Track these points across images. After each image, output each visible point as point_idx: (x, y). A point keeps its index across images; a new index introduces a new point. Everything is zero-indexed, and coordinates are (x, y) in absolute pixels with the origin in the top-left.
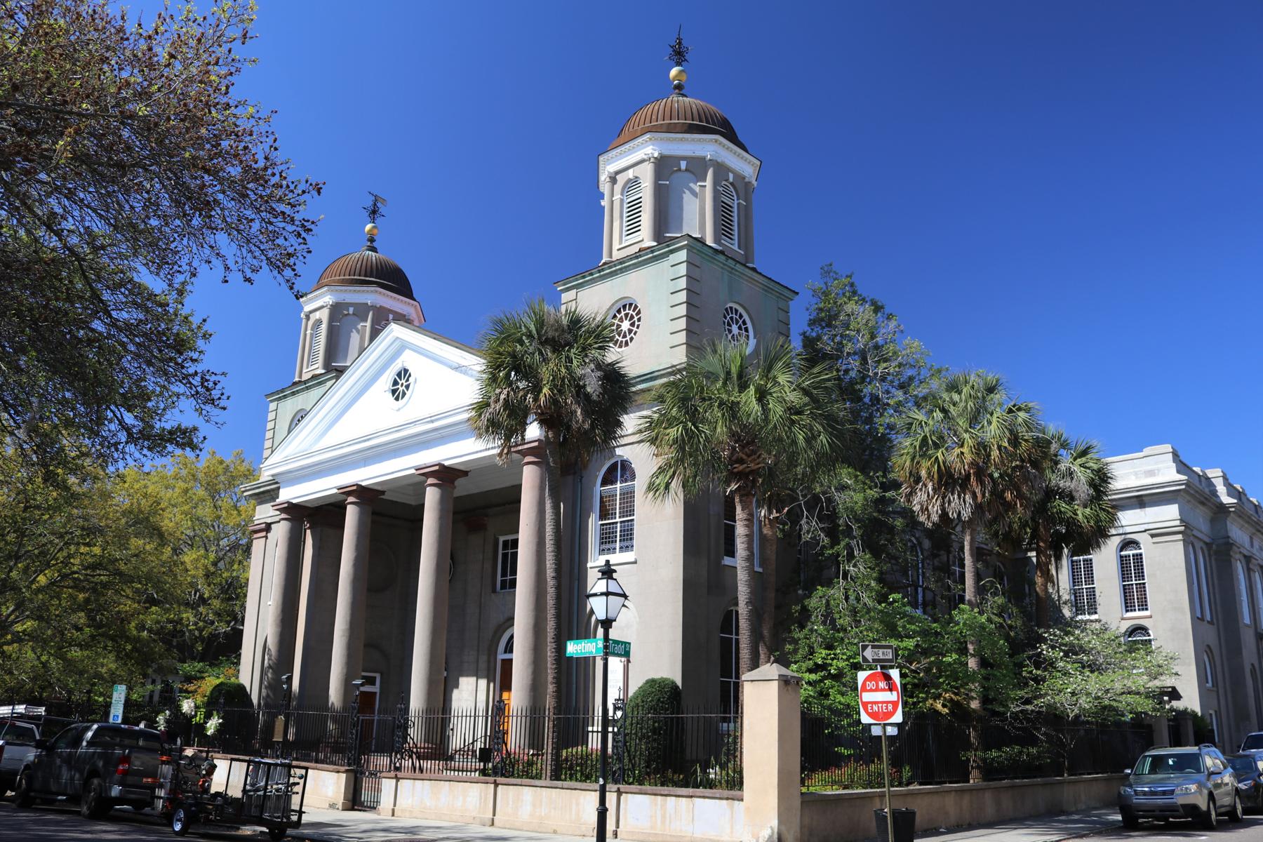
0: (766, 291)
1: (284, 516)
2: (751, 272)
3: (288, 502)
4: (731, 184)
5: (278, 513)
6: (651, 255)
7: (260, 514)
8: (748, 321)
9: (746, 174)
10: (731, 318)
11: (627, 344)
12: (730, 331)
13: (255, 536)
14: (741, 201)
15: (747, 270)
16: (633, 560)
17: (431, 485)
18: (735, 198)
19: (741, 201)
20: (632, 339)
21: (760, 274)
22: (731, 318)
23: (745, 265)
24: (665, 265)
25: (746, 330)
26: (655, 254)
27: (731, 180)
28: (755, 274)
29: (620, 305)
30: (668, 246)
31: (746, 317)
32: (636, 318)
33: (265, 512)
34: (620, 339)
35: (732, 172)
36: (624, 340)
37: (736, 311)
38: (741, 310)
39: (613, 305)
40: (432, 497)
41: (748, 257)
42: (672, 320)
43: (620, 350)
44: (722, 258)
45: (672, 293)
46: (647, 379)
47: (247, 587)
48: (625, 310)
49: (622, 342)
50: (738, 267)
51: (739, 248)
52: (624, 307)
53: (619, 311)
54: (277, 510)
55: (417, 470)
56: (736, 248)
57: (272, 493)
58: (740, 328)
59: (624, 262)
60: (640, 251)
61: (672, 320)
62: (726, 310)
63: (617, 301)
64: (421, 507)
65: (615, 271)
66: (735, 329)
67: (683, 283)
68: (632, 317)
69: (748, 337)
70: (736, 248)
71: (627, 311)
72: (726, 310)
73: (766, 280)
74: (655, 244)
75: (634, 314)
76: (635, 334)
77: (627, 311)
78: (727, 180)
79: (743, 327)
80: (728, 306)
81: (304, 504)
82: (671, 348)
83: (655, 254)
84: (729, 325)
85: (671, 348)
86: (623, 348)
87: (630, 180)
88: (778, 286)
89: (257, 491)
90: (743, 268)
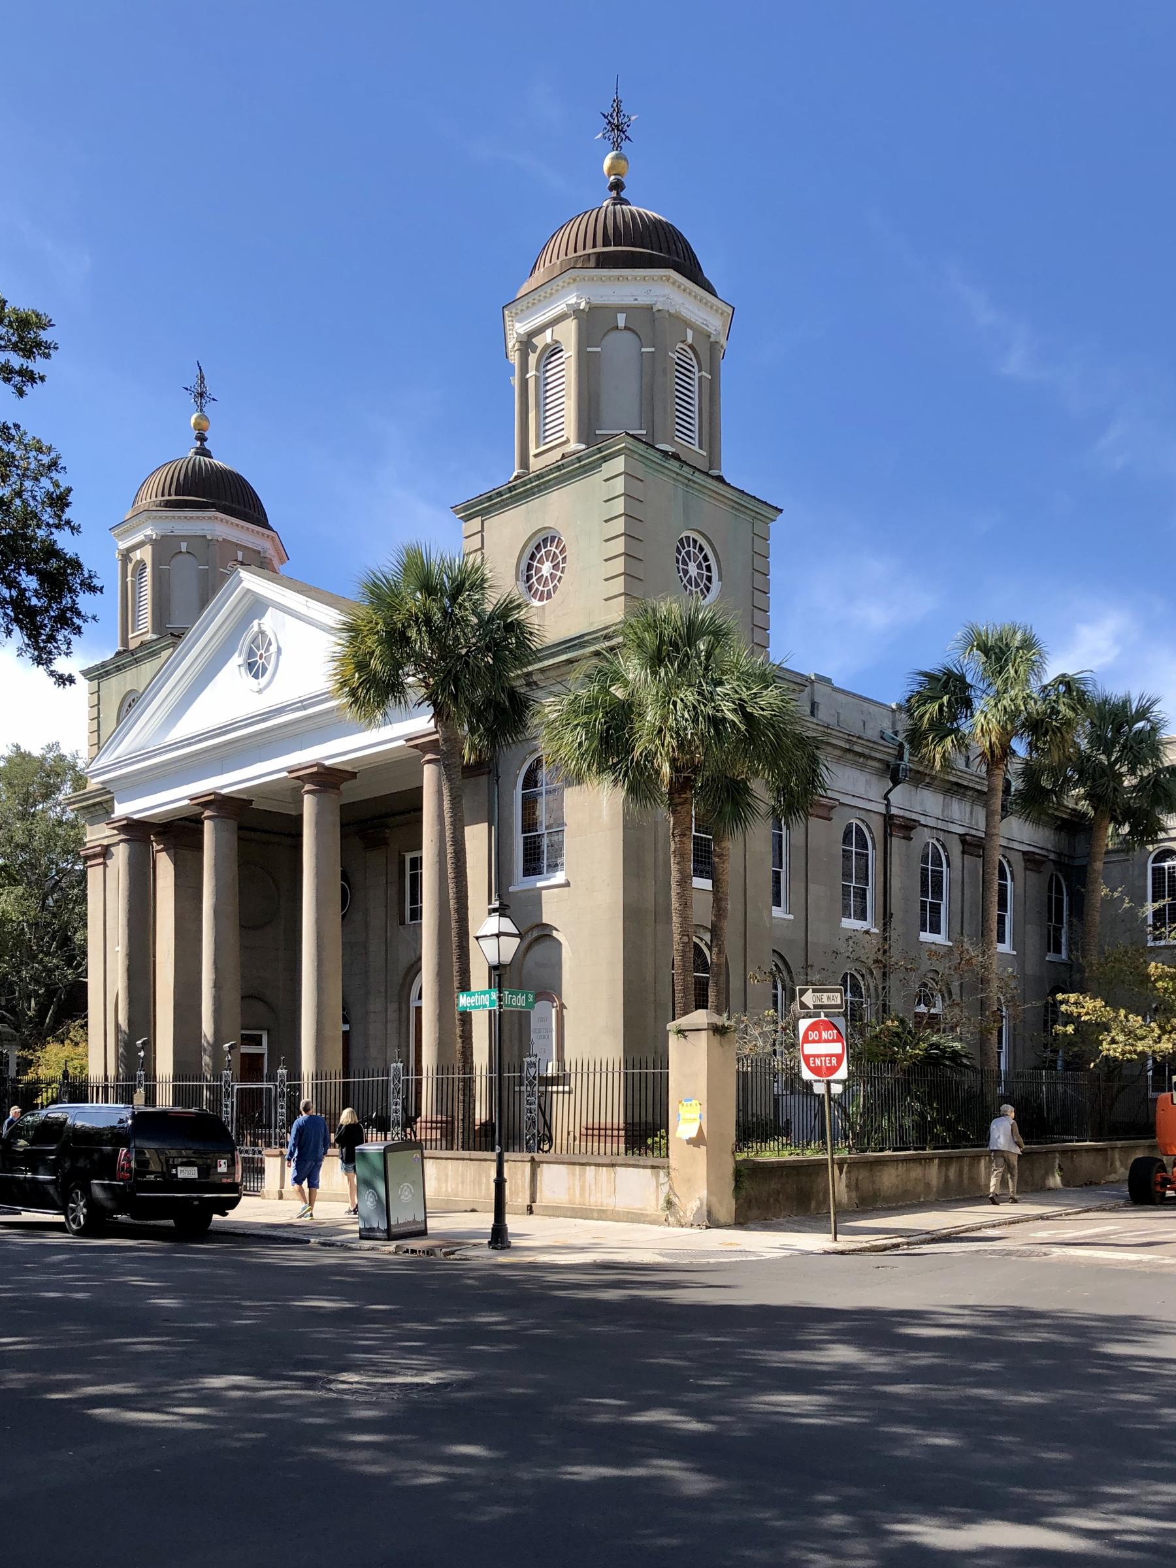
0: (737, 510)
1: (123, 837)
2: (715, 483)
3: (126, 818)
4: (691, 346)
5: (116, 832)
6: (578, 465)
7: (92, 834)
8: (711, 556)
9: (711, 329)
10: (688, 553)
11: (549, 596)
12: (686, 572)
13: (89, 863)
14: (704, 373)
15: (710, 480)
16: (563, 881)
17: (308, 792)
18: (696, 370)
19: (704, 373)
20: (555, 587)
21: (728, 485)
22: (688, 553)
23: (706, 474)
24: (596, 478)
25: (709, 569)
26: (582, 463)
27: (690, 341)
28: (721, 486)
29: (538, 539)
30: (600, 450)
31: (708, 550)
32: (560, 558)
33: (97, 834)
34: (541, 588)
35: (692, 328)
36: (546, 589)
37: (695, 541)
38: (701, 541)
39: (530, 539)
40: (309, 805)
41: (713, 458)
42: (606, 560)
43: (541, 603)
44: (673, 465)
45: (606, 521)
46: (575, 645)
47: (85, 926)
48: (545, 547)
49: (543, 592)
50: (698, 477)
51: (701, 448)
52: (545, 540)
53: (538, 548)
54: (114, 828)
55: (290, 772)
56: (696, 448)
57: (105, 805)
58: (699, 567)
59: (543, 478)
60: (563, 456)
61: (606, 560)
62: (681, 541)
63: (535, 534)
64: (301, 816)
65: (531, 489)
66: (693, 570)
67: (619, 506)
68: (555, 556)
69: (709, 579)
70: (696, 448)
71: (549, 548)
72: (681, 541)
73: (737, 494)
74: (583, 447)
75: (557, 552)
76: (559, 581)
77: (549, 548)
78: (683, 342)
79: (704, 565)
80: (683, 535)
81: (146, 820)
82: (606, 600)
83: (582, 463)
84: (685, 563)
85: (606, 600)
86: (545, 602)
87: (547, 346)
88: (753, 502)
89: (85, 804)
90: (702, 477)
